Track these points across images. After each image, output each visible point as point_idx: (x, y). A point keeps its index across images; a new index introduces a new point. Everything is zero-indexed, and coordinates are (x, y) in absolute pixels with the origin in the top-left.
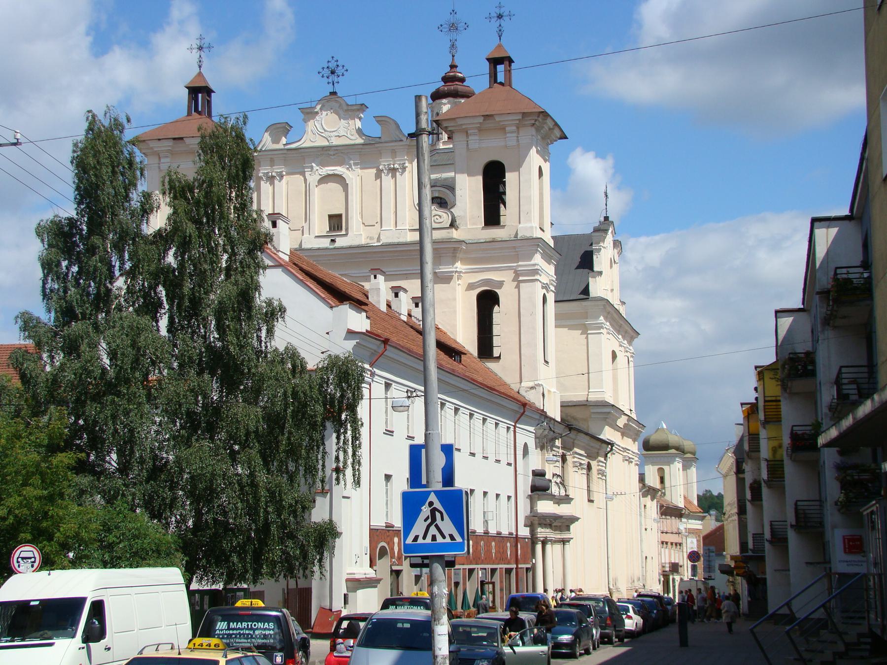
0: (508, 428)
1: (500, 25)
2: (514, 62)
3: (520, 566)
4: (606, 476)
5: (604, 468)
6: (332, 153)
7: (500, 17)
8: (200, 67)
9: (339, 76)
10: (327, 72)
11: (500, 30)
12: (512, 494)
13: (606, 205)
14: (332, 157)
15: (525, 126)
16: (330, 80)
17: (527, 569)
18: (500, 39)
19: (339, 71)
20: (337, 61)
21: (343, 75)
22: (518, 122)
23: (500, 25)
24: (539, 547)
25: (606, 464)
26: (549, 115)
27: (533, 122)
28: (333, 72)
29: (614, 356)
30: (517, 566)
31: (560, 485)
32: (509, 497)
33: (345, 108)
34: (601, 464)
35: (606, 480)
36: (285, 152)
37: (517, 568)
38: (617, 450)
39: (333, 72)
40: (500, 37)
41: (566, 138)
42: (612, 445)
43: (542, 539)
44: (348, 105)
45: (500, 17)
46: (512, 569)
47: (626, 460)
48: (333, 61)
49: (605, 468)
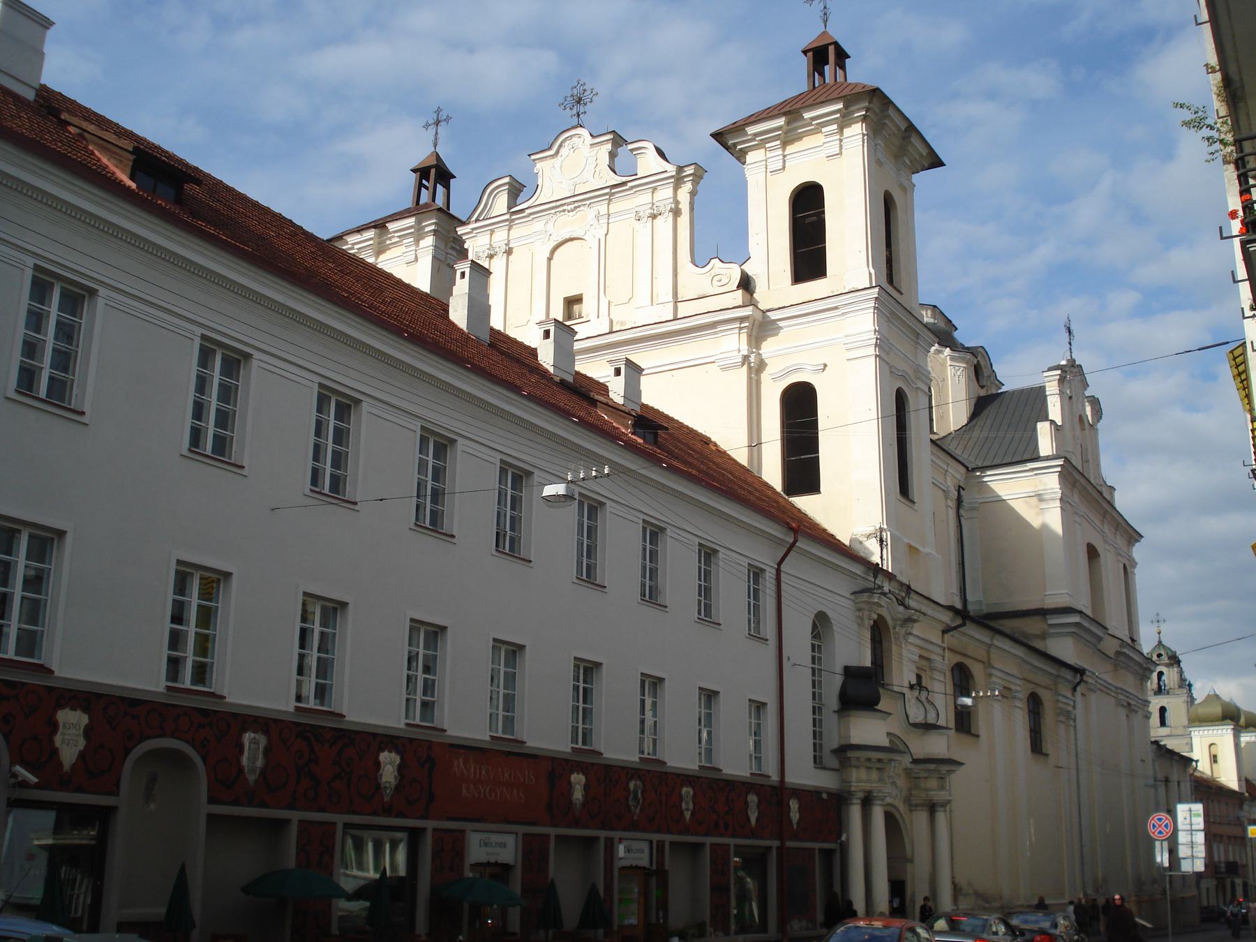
0: (756, 573)
1: (825, 8)
2: (849, 57)
3: (790, 844)
4: (1075, 720)
5: (1070, 708)
6: (569, 208)
9: (586, 104)
11: (825, 14)
12: (771, 700)
13: (1070, 344)
14: (571, 214)
16: (575, 111)
17: (827, 854)
18: (826, 27)
20: (585, 84)
21: (591, 102)
23: (825, 8)
24: (855, 812)
25: (1074, 701)
29: (1092, 552)
31: (926, 704)
32: (759, 707)
34: (1061, 699)
35: (1075, 727)
37: (780, 849)
38: (1104, 689)
39: (579, 101)
40: (825, 22)
41: (941, 164)
42: (1080, 671)
46: (769, 848)
47: (1123, 706)
49: (1074, 707)
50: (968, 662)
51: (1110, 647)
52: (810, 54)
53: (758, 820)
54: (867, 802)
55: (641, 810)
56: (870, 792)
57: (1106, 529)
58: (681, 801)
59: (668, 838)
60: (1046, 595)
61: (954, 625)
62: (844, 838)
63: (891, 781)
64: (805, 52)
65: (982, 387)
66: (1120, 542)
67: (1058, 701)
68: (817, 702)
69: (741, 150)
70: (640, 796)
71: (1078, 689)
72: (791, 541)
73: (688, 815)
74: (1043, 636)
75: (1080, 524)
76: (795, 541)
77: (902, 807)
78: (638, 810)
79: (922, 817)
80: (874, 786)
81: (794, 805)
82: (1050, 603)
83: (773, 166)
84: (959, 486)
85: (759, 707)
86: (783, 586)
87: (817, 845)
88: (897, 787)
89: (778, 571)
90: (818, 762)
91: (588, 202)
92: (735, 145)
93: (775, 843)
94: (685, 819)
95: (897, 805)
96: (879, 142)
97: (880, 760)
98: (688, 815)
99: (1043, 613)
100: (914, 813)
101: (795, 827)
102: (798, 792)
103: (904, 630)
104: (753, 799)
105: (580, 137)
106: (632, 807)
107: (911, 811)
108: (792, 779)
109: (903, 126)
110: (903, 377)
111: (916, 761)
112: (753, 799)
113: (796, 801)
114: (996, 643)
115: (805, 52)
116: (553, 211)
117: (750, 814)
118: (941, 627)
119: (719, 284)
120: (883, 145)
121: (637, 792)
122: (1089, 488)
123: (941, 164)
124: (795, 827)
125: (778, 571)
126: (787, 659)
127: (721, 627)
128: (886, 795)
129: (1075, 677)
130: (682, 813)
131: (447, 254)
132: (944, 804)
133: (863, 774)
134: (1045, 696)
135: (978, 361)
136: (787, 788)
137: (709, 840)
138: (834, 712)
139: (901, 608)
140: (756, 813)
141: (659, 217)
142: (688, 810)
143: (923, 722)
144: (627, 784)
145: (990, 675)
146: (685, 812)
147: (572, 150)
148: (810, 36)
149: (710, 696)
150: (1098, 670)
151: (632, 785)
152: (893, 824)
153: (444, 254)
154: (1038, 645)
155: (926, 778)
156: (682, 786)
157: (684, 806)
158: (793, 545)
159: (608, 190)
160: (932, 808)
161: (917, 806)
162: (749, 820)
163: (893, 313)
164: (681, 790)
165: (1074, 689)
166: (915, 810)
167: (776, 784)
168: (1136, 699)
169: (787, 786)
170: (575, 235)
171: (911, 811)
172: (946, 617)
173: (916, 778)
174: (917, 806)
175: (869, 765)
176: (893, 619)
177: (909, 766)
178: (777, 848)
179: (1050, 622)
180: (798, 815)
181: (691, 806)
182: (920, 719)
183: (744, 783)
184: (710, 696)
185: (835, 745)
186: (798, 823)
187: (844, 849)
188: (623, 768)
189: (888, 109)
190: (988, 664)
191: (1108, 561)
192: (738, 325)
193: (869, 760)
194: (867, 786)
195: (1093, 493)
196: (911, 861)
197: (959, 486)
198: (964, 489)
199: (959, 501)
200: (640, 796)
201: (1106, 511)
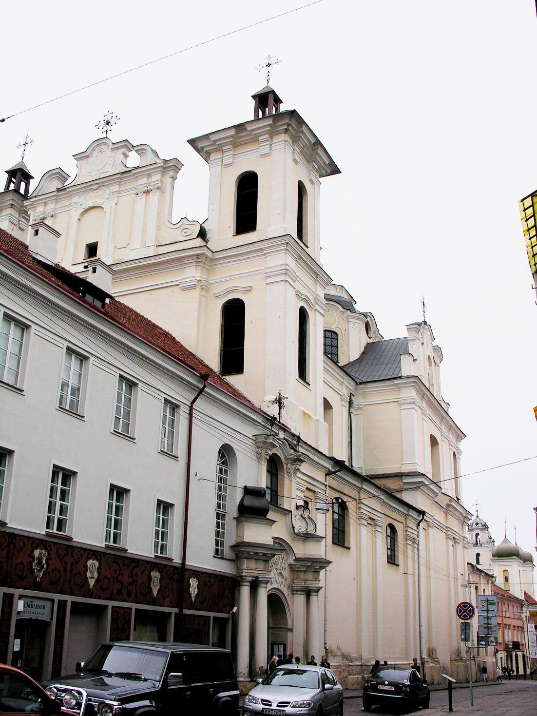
3: (186, 611)
5: (416, 537)
6: (94, 187)
7: (269, 65)
8: (23, 158)
10: (103, 124)
12: (178, 502)
14: (95, 192)
15: (278, 133)
16: (104, 130)
19: (112, 122)
22: (269, 128)
26: (304, 122)
27: (286, 127)
28: (108, 123)
29: (434, 442)
30: (181, 611)
31: (308, 520)
32: (164, 507)
33: (111, 146)
36: (55, 193)
39: (108, 123)
41: (339, 172)
42: (423, 513)
43: (250, 579)
44: (113, 144)
45: (269, 65)
48: (109, 114)
50: (345, 499)
51: (444, 501)
52: (257, 99)
53: (159, 591)
54: (255, 585)
55: (45, 574)
56: (257, 578)
57: (443, 427)
58: (86, 570)
59: (70, 599)
60: (403, 464)
61: (333, 470)
62: (235, 610)
63: (278, 572)
64: (254, 97)
65: (370, 338)
66: (452, 438)
67: (407, 531)
68: (221, 510)
69: (206, 152)
70: (44, 562)
71: (421, 524)
72: (201, 386)
73: (92, 582)
74: (399, 491)
75: (426, 422)
76: (204, 387)
77: (286, 591)
78: (41, 574)
79: (301, 599)
80: (262, 575)
81: (194, 583)
82: (405, 469)
83: (226, 161)
84: (351, 394)
85: (164, 507)
86: (194, 420)
87: (212, 614)
88: (283, 577)
89: (191, 408)
90: (218, 554)
91: (106, 184)
92: (202, 148)
93: (174, 610)
94: (89, 585)
95: (281, 589)
96: (296, 148)
97: (265, 554)
98: (92, 582)
99: (399, 476)
100: (295, 596)
101: (193, 599)
102: (197, 573)
103: (294, 467)
104: (155, 575)
105: (105, 145)
106: (36, 571)
107: (293, 594)
108: (192, 562)
109: (313, 141)
110: (306, 300)
111: (297, 560)
112: (155, 575)
113: (195, 580)
114: (364, 487)
115: (254, 97)
116: (84, 190)
117: (152, 586)
118: (326, 471)
119: (186, 234)
120: (299, 151)
121: (42, 558)
122: (433, 400)
123: (339, 172)
124: (193, 599)
125: (191, 408)
126: (195, 474)
127: (135, 441)
128: (269, 580)
129: (419, 517)
130: (86, 580)
131: (19, 221)
132: (317, 590)
133: (252, 564)
134: (399, 527)
135: (367, 321)
136: (188, 570)
137: (111, 604)
138: (234, 518)
139: (292, 451)
140: (158, 587)
141: (151, 192)
142: (92, 578)
143: (305, 532)
144: (32, 552)
145: (360, 508)
146: (90, 580)
147: (100, 153)
148: (259, 88)
149: (119, 493)
150: (435, 513)
151: (37, 553)
152: (276, 603)
153: (18, 221)
154: (398, 495)
155: (305, 571)
156: (88, 559)
157: (88, 574)
158: (202, 390)
159: (119, 176)
160: (308, 593)
161: (297, 591)
162: (151, 590)
163: (300, 256)
164: (86, 562)
165: (418, 525)
166: (295, 594)
167: (179, 566)
168: (458, 535)
169: (186, 567)
170: (97, 204)
171: (293, 594)
172: (328, 465)
173: (297, 571)
174: (297, 591)
175: (256, 557)
176: (286, 459)
177: (293, 562)
178: (175, 613)
179: (404, 481)
180: (196, 591)
181: (96, 575)
182: (303, 530)
183: (148, 562)
184: (119, 493)
185: (233, 543)
186: (197, 596)
187: (235, 618)
188: (29, 538)
189: (302, 127)
190: (359, 501)
191: (444, 449)
192: (195, 260)
193: (256, 554)
194: (255, 573)
195: (436, 403)
196: (291, 630)
197: (351, 394)
198: (353, 396)
199: (351, 403)
200: (44, 562)
201: (443, 417)
